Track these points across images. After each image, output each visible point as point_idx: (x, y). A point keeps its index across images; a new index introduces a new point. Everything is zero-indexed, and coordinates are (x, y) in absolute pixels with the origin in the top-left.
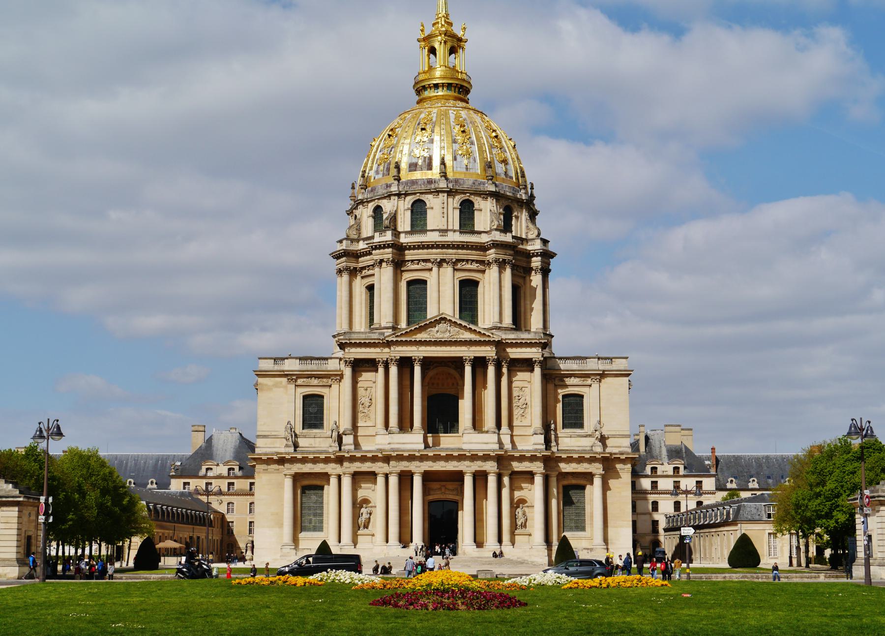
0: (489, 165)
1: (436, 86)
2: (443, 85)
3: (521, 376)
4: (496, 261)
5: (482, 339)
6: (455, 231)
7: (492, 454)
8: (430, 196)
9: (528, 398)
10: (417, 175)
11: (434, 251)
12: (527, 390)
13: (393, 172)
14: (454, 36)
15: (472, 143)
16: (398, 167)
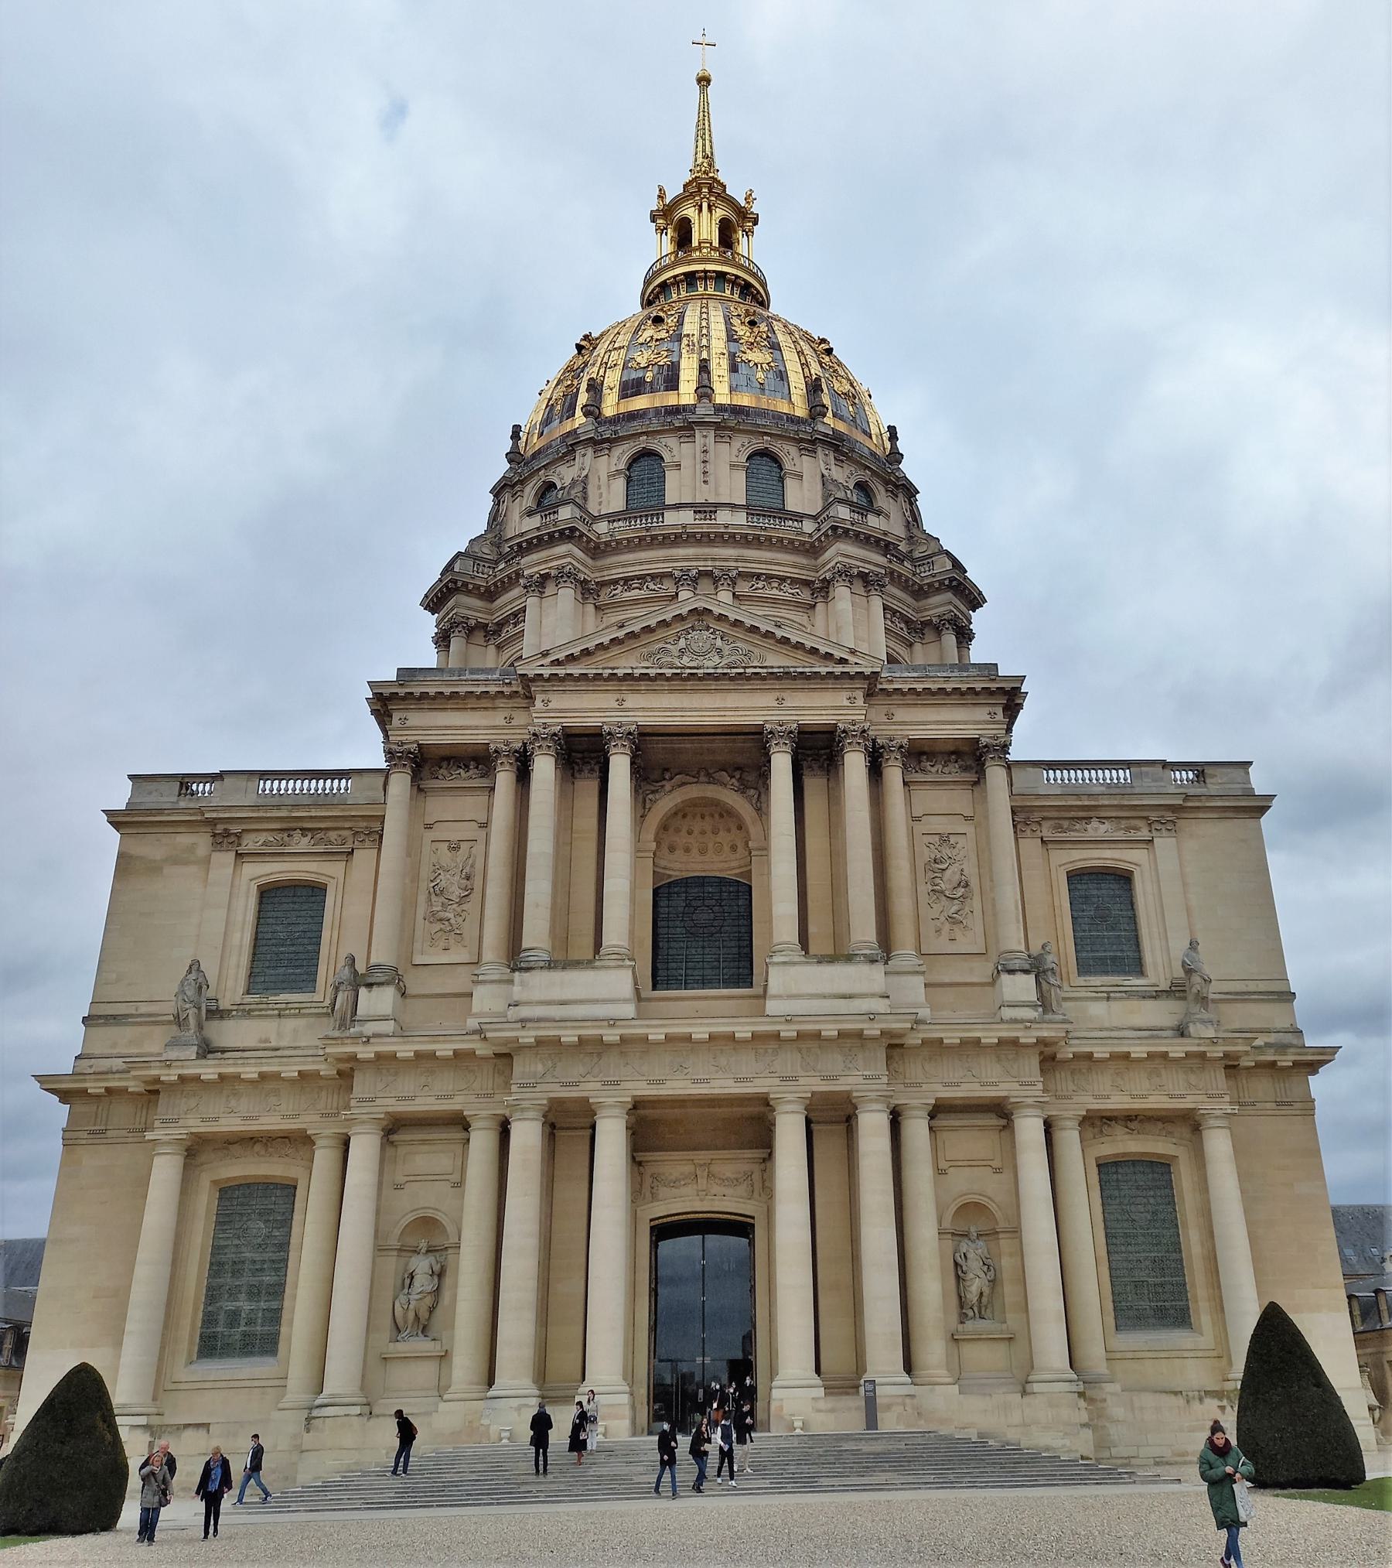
0: (814, 387)
1: (691, 279)
2: (706, 276)
3: (942, 799)
4: (845, 573)
5: (823, 670)
6: (733, 507)
7: (872, 1030)
8: (672, 441)
9: (971, 871)
10: (640, 403)
11: (681, 552)
12: (966, 846)
13: (583, 398)
14: (731, 202)
15: (775, 347)
16: (595, 388)
